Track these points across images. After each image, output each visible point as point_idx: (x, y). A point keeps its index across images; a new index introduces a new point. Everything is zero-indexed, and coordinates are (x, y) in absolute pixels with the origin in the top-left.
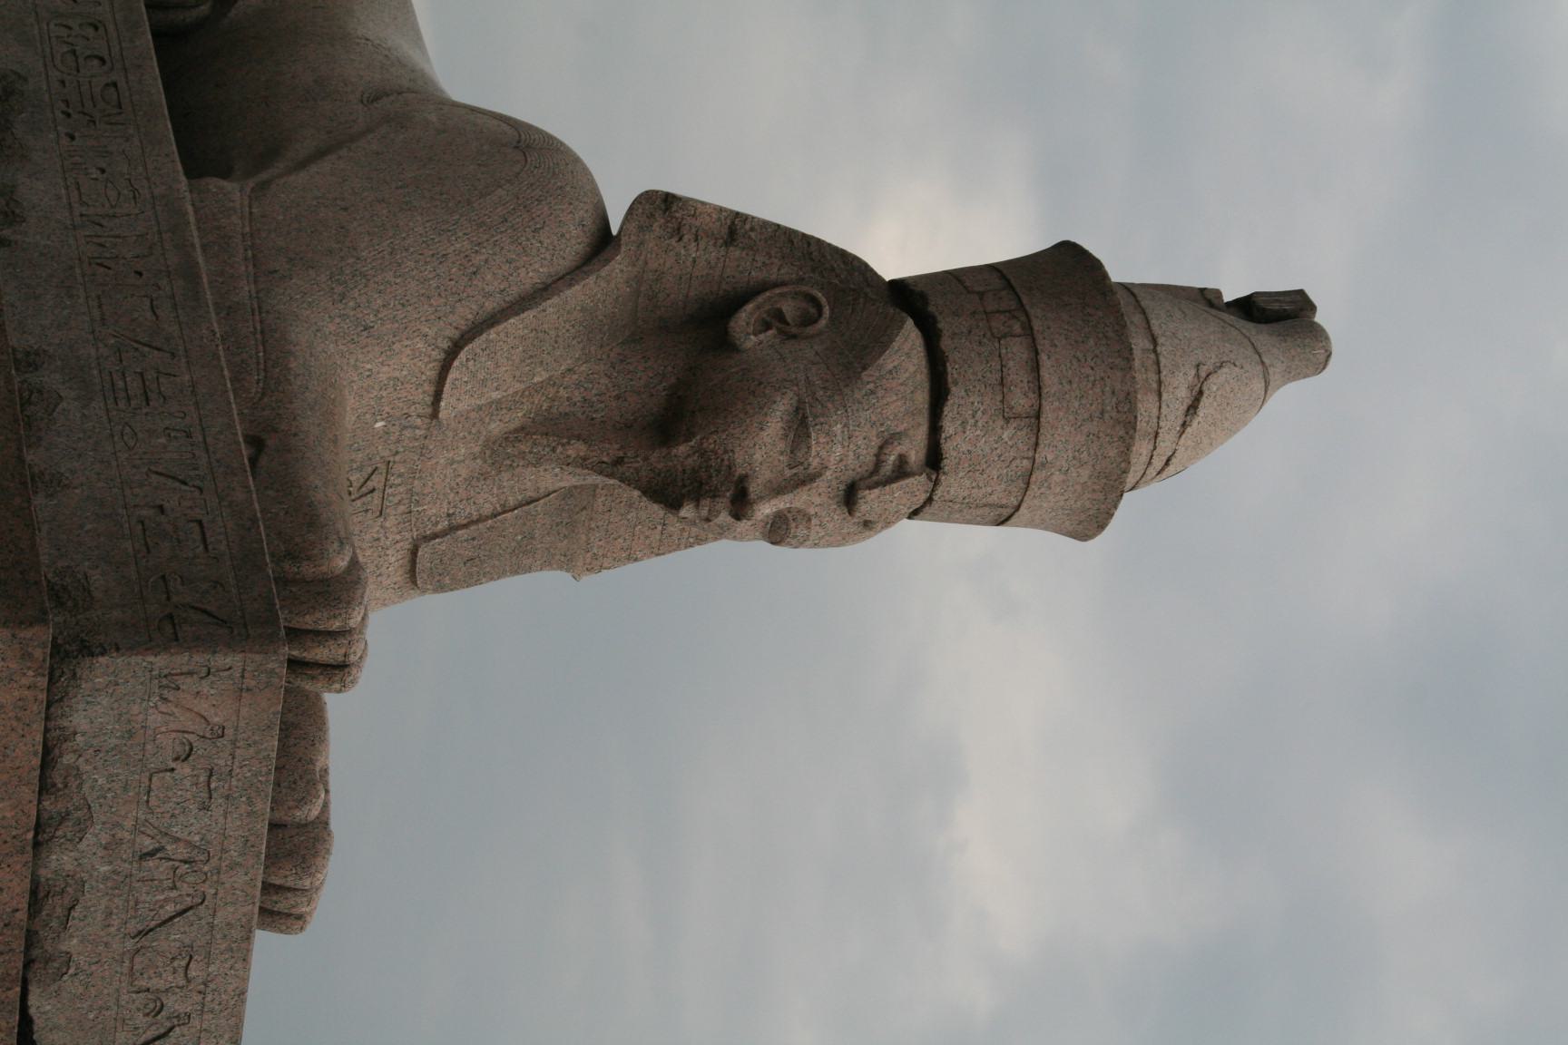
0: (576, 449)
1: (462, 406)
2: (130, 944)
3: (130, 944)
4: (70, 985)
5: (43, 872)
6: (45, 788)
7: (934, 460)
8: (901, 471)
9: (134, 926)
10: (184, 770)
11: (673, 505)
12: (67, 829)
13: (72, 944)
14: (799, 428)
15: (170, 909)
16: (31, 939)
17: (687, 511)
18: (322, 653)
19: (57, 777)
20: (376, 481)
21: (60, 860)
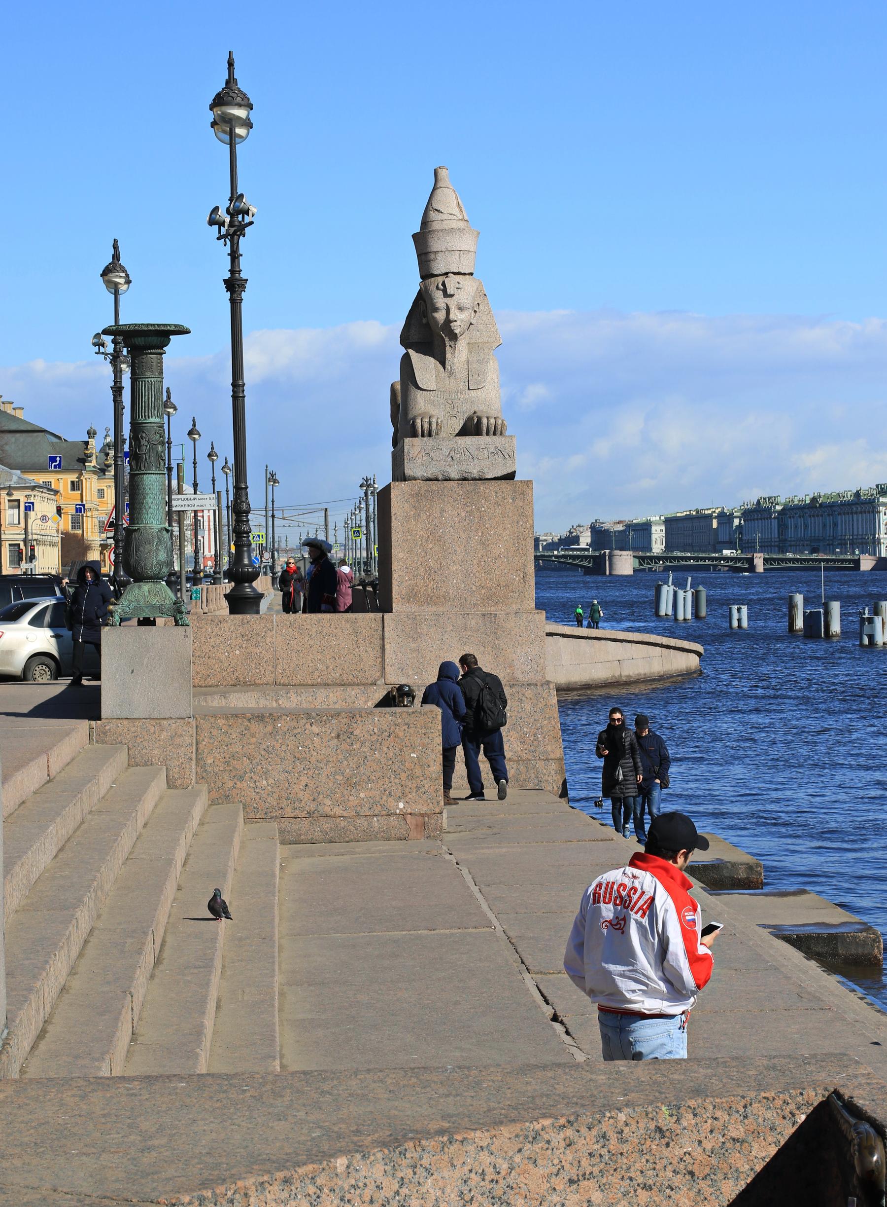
0: (448, 356)
1: (434, 384)
2: (476, 460)
3: (476, 460)
4: (486, 470)
5: (457, 477)
6: (437, 480)
7: (446, 274)
8: (444, 284)
9: (471, 460)
10: (431, 454)
11: (456, 334)
12: (446, 474)
13: (475, 471)
14: (436, 310)
15: (467, 453)
16: (474, 479)
17: (457, 331)
18: (426, 426)
19: (432, 477)
20: (450, 401)
21: (454, 475)
